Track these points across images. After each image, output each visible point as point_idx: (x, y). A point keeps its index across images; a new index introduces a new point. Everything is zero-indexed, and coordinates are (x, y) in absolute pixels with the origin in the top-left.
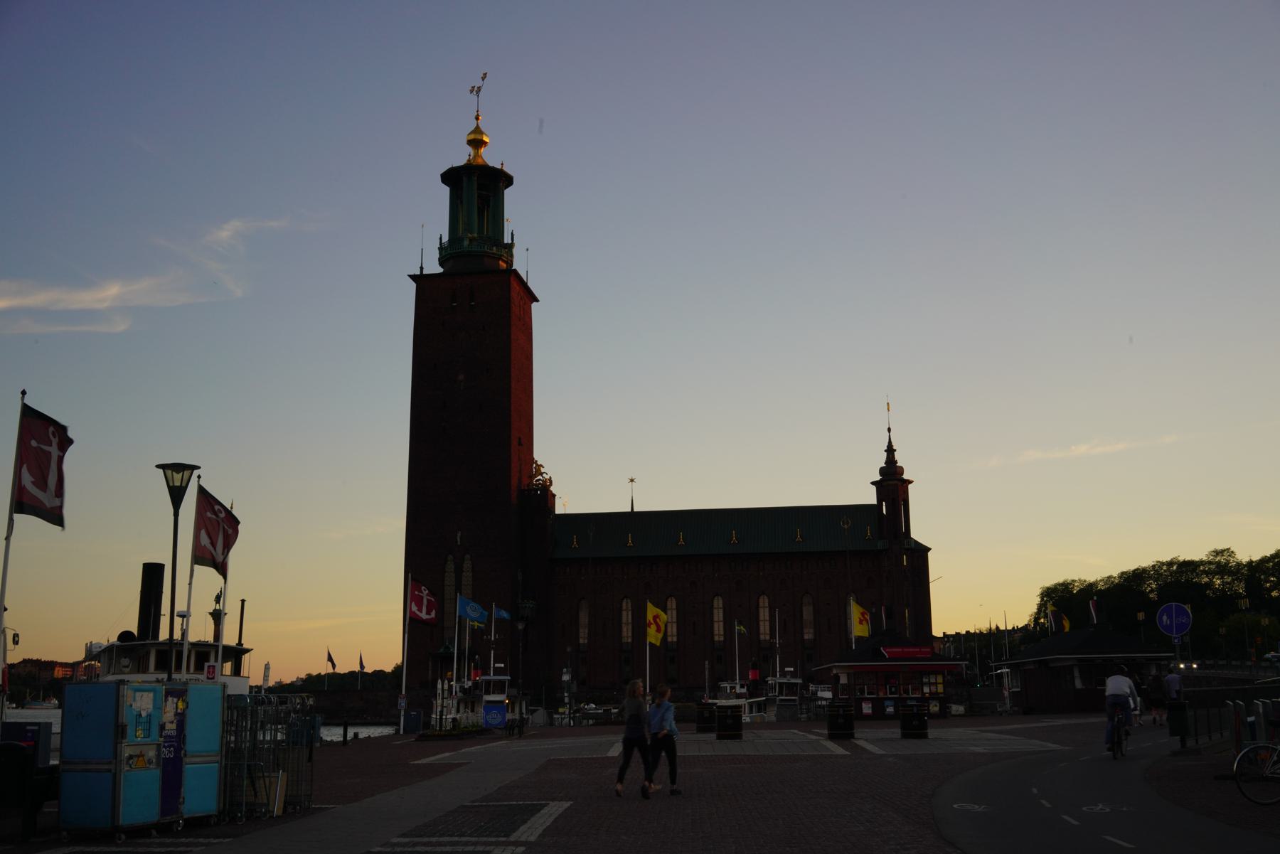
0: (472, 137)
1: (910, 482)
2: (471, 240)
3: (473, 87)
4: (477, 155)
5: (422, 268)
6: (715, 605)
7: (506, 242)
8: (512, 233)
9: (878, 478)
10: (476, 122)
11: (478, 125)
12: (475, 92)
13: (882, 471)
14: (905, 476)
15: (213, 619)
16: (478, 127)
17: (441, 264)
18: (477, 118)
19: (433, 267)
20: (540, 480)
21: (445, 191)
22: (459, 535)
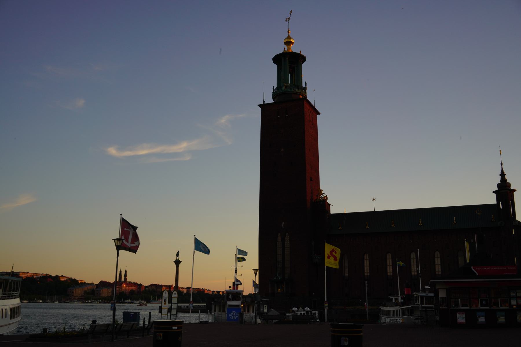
0: (286, 41)
1: (515, 191)
2: (286, 87)
3: (287, 19)
4: (289, 49)
5: (264, 101)
6: (412, 257)
7: (303, 87)
8: (306, 83)
9: (497, 189)
10: (288, 33)
11: (289, 35)
12: (287, 21)
13: (499, 185)
14: (512, 188)
15: (176, 264)
16: (289, 36)
17: (274, 100)
18: (289, 32)
19: (269, 100)
20: (322, 197)
21: (275, 66)
22: (283, 224)
